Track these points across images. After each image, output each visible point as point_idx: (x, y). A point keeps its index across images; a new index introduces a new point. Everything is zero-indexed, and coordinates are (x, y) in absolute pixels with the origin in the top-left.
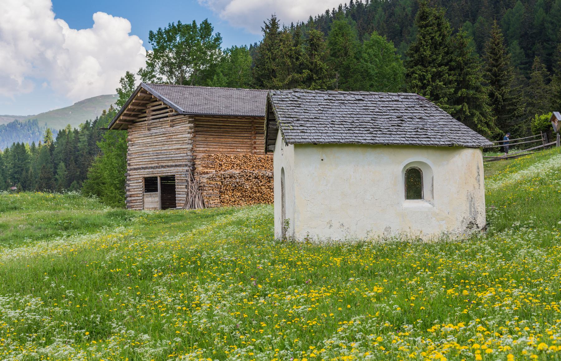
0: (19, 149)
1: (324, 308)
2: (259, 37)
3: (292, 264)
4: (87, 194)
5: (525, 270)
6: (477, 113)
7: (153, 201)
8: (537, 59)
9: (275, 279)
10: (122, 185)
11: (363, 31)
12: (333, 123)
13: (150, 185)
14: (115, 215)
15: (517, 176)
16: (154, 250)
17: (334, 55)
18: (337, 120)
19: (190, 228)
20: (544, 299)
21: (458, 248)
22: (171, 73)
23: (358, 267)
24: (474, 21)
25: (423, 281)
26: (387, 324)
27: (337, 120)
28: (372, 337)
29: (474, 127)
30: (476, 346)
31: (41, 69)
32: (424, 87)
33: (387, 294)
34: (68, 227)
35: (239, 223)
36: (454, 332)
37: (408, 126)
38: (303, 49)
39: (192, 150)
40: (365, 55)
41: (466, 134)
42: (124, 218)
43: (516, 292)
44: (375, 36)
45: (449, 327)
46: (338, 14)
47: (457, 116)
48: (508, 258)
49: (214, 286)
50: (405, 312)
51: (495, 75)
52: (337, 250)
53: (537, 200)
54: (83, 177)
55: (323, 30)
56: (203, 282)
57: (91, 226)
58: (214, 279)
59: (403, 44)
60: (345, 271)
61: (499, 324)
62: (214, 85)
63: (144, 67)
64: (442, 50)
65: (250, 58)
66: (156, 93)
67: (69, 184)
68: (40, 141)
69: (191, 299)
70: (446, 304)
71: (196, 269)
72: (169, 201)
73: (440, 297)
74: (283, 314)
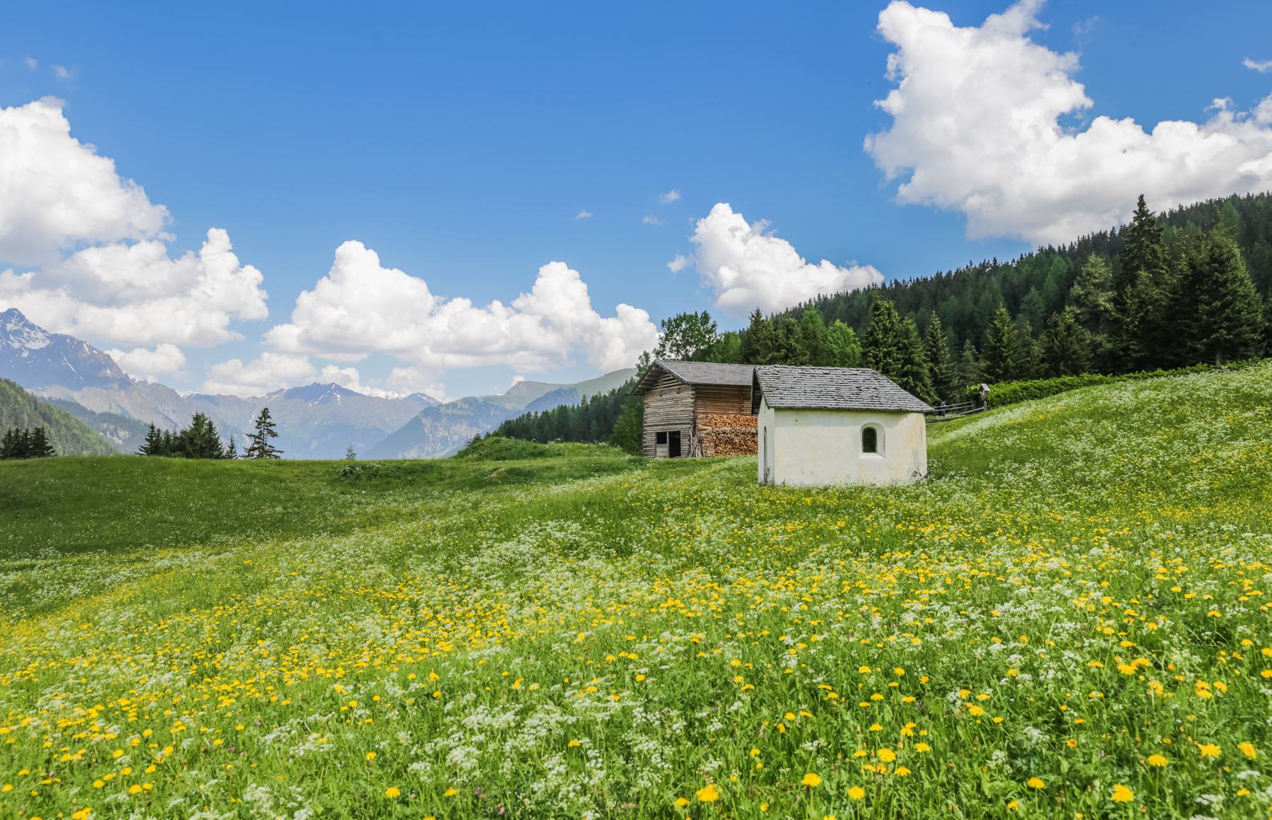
0: (563, 409)
1: (798, 538)
2: (746, 325)
3: (773, 503)
4: (613, 445)
5: (959, 511)
7: (663, 450)
8: (968, 342)
9: (759, 514)
11: (828, 321)
12: (805, 392)
15: (952, 435)
16: (665, 489)
19: (691, 472)
20: (974, 533)
21: (904, 492)
23: (824, 506)
24: (917, 311)
25: (877, 518)
26: (848, 551)
28: (836, 561)
29: (918, 396)
30: (920, 571)
31: (581, 349)
32: (877, 363)
34: (599, 470)
35: (730, 469)
36: (902, 560)
37: (865, 395)
38: (780, 333)
41: (912, 402)
42: (640, 464)
43: (952, 528)
44: (838, 323)
45: (898, 555)
46: (808, 307)
47: (904, 386)
48: (945, 501)
49: (712, 518)
50: (862, 543)
51: (934, 354)
52: (808, 493)
53: (968, 454)
54: (610, 431)
56: (703, 515)
57: (616, 470)
59: (860, 329)
60: (814, 508)
61: (939, 553)
62: (711, 361)
63: (658, 347)
65: (739, 341)
66: (667, 367)
67: (599, 437)
70: (896, 536)
71: (696, 505)
73: (891, 531)
74: (766, 542)
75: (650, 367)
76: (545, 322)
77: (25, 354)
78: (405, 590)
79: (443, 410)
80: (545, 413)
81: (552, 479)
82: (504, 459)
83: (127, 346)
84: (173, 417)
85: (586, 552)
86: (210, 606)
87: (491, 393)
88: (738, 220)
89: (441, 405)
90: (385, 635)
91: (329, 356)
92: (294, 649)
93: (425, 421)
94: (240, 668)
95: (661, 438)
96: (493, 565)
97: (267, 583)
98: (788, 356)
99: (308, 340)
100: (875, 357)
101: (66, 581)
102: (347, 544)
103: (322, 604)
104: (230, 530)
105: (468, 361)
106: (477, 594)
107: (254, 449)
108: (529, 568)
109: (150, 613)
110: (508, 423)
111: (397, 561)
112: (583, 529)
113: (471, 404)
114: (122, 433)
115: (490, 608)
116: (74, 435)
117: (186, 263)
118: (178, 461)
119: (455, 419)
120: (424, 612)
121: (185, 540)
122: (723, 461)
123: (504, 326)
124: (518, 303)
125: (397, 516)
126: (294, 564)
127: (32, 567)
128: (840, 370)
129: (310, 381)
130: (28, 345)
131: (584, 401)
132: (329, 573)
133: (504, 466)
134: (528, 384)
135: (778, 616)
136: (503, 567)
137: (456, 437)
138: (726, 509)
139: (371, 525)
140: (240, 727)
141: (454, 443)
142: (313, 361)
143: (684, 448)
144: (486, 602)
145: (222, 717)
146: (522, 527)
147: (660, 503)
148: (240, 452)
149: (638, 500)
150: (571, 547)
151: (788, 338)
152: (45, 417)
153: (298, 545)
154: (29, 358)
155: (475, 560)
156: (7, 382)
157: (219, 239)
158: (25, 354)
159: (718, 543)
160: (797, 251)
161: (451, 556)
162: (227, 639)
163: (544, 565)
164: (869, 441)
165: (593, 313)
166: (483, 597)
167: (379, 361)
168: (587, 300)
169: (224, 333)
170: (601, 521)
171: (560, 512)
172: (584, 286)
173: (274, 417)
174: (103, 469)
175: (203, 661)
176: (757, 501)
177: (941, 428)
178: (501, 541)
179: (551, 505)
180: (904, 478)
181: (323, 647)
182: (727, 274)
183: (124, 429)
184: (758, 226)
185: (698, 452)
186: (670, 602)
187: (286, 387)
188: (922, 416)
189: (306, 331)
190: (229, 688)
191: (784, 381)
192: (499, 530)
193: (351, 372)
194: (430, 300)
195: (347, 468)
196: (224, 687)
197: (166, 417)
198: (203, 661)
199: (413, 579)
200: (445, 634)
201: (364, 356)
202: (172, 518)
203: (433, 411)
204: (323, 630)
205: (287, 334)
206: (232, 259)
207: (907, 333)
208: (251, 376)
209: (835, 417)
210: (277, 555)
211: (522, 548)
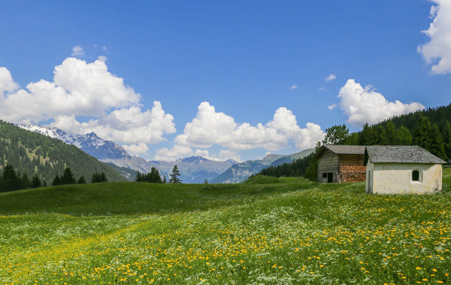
1: (383, 215)
2: (361, 129)
3: (372, 201)
6: (439, 152)
7: (326, 180)
9: (366, 205)
10: (316, 176)
12: (388, 156)
13: (325, 175)
14: (314, 184)
16: (327, 195)
17: (387, 134)
18: (389, 155)
22: (332, 141)
23: (394, 202)
27: (389, 155)
31: (292, 142)
33: (405, 211)
35: (353, 187)
37: (415, 157)
39: (338, 165)
40: (398, 134)
41: (435, 159)
42: (317, 186)
44: (402, 127)
46: (389, 121)
47: (432, 153)
50: (412, 217)
51: (447, 139)
52: (387, 196)
55: (383, 126)
56: (343, 205)
57: (306, 187)
58: (346, 204)
60: (390, 203)
62: (346, 145)
63: (324, 140)
64: (427, 131)
67: (299, 175)
68: (291, 162)
69: (339, 210)
70: (428, 215)
71: (340, 201)
72: (330, 180)
74: (369, 216)
75: (321, 148)
76: (279, 131)
78: (228, 230)
79: (239, 166)
80: (278, 166)
81: (282, 191)
82: (263, 183)
83: (129, 144)
84: (144, 169)
85: (296, 218)
86: (161, 233)
87: (257, 159)
88: (358, 86)
89: (238, 164)
90: (222, 246)
91: (198, 146)
92: (190, 249)
93: (233, 170)
94: (172, 255)
95: (325, 175)
96: (260, 222)
97: (180, 226)
98: (379, 142)
99: (189, 140)
100: (419, 141)
101: (115, 223)
102: (207, 214)
103: (199, 234)
104: (166, 208)
105: (249, 147)
106: (254, 233)
107: (172, 180)
108: (274, 224)
109: (142, 235)
110: (264, 170)
111: (225, 220)
112: (295, 210)
113: (250, 163)
114: (128, 174)
115: (260, 238)
116: (113, 175)
117: (147, 113)
118: (147, 184)
119: (244, 169)
120: (236, 238)
121: (151, 211)
122: (350, 184)
123: (263, 132)
124: (268, 125)
125: (224, 204)
126: (189, 221)
127: (104, 218)
128: (403, 147)
129: (191, 155)
131: (294, 161)
132: (201, 224)
133: (263, 186)
134: (272, 155)
135: (377, 246)
136: (264, 223)
137: (244, 176)
138: (353, 203)
139: (214, 207)
140: (175, 275)
141: (244, 178)
142: (192, 148)
143: (334, 179)
144: (258, 236)
145: (169, 271)
146: (271, 209)
147: (325, 201)
148: (168, 181)
149: (316, 199)
150: (290, 216)
151: (379, 134)
152: (104, 169)
153: (189, 214)
155: (254, 220)
156: (92, 157)
157: (157, 104)
158: (97, 148)
159: (350, 216)
160: (385, 97)
161: (245, 218)
162: (168, 245)
163: (280, 223)
164: (416, 176)
165: (298, 127)
166: (257, 234)
167: (216, 148)
168: (296, 122)
169: (161, 138)
170: (302, 207)
171: (286, 203)
172: (295, 117)
173: (179, 169)
174: (123, 186)
175: (160, 252)
176: (366, 200)
177: (449, 170)
178: (263, 214)
179: (282, 201)
180: (431, 191)
181: (200, 249)
182: (353, 109)
183: (129, 173)
184: (367, 88)
185: (340, 181)
186: (331, 238)
187: (183, 157)
188: (440, 166)
189: (189, 137)
190: (170, 261)
191: (378, 152)
192: (262, 210)
193: (206, 152)
194: (235, 124)
195: (205, 187)
196: (168, 261)
197: (142, 169)
198: (160, 252)
199: (231, 227)
200: (244, 247)
201: (210, 146)
202: (146, 203)
203: (236, 166)
204: (200, 243)
205: (182, 138)
206: (162, 112)
207: (434, 131)
208: (170, 154)
209: (401, 166)
210: (183, 217)
211: (271, 216)
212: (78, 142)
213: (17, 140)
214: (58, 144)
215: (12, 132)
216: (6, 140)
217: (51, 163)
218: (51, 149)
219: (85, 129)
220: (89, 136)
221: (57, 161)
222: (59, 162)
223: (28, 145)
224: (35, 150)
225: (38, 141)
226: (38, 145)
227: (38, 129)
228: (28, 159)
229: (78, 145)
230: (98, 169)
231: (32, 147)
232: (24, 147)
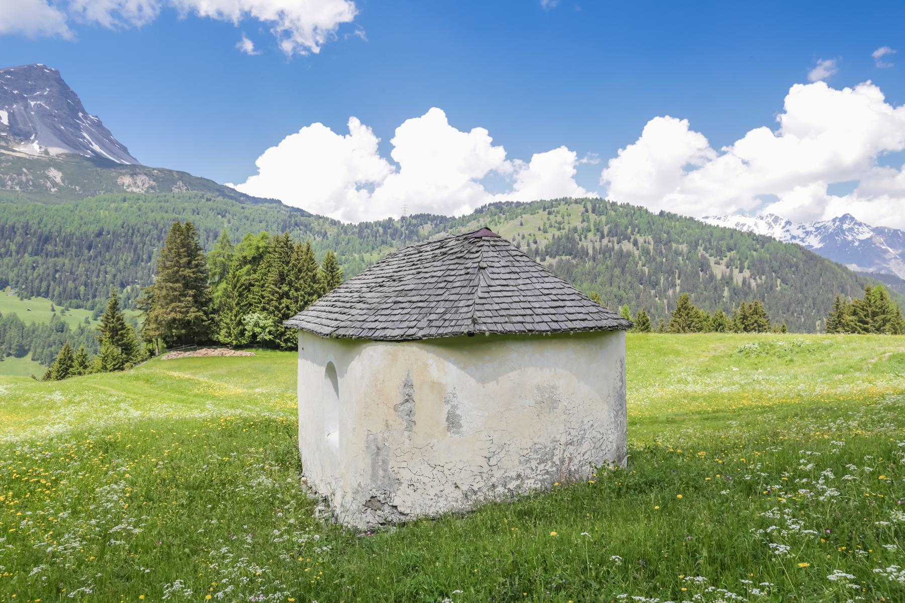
77: (856, 244)
130: (858, 237)
154: (859, 246)
156: (837, 264)
212: (816, 236)
213: (697, 245)
214: (766, 245)
215: (690, 231)
216: (680, 246)
217: (752, 281)
218: (752, 256)
219: (837, 207)
220: (837, 223)
221: (764, 277)
222: (767, 277)
223: (714, 252)
224: (725, 259)
225: (732, 242)
226: (730, 250)
227: (742, 220)
228: (712, 277)
229: (814, 243)
230: (849, 287)
231: (720, 253)
232: (707, 255)
